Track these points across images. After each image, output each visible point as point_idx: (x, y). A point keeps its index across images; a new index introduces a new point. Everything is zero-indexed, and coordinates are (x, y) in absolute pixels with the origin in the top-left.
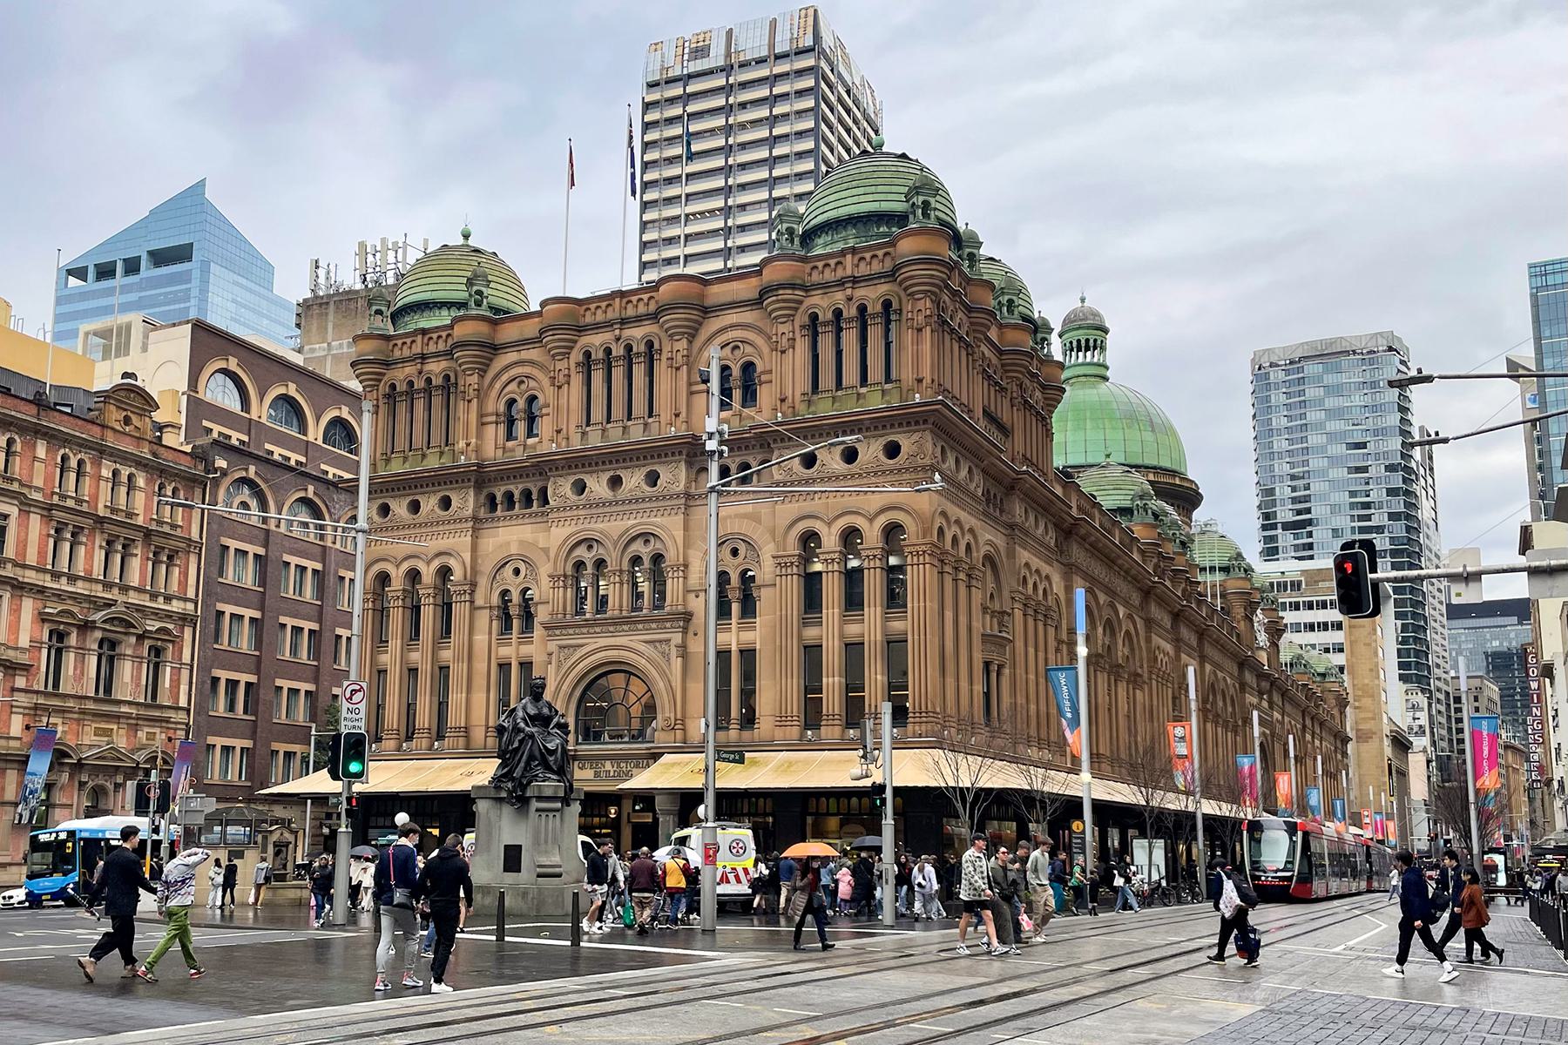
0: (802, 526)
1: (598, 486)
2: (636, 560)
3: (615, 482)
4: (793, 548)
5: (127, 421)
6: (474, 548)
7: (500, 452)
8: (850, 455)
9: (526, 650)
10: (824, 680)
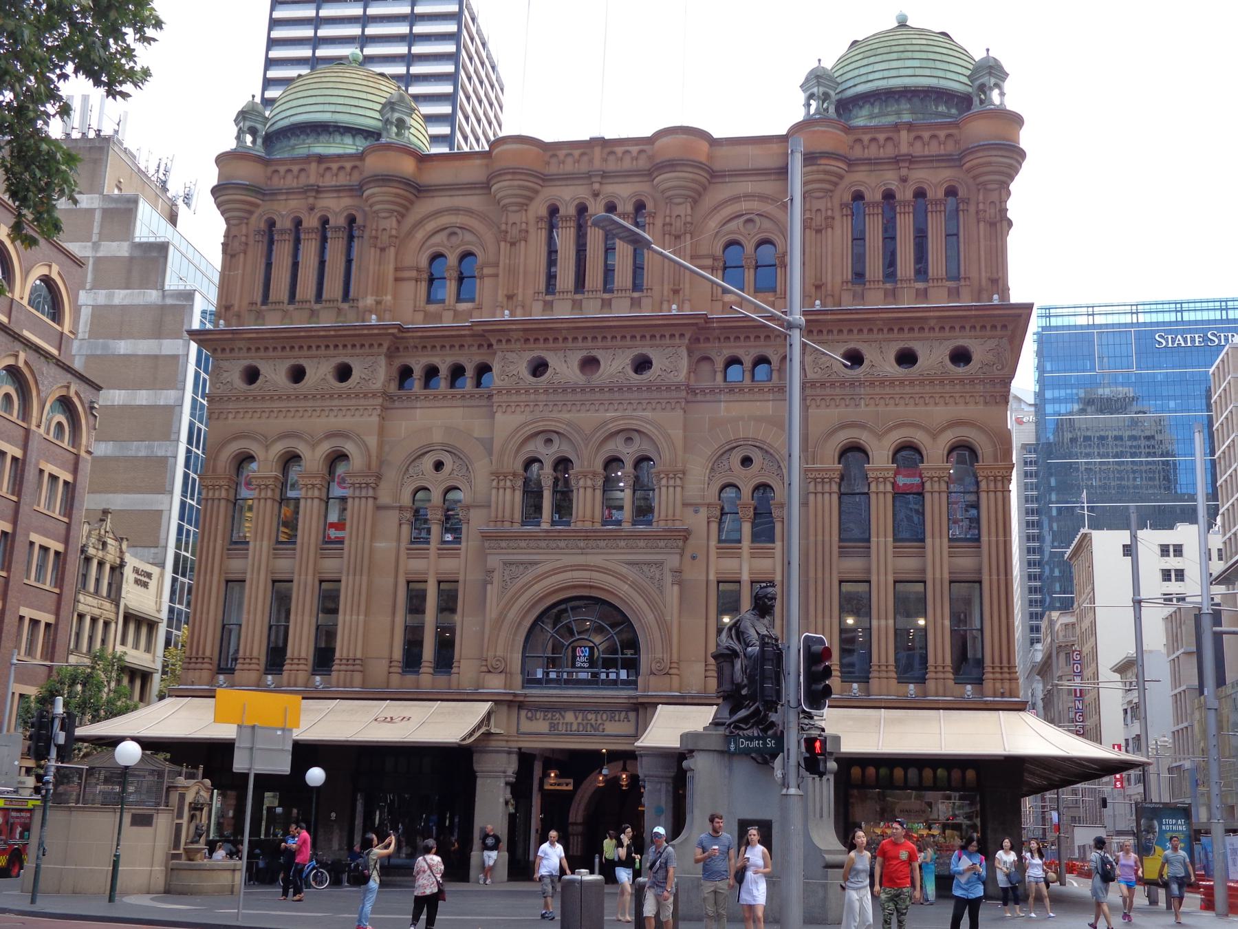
0: (843, 437)
2: (613, 462)
3: (590, 364)
4: (829, 462)
6: (382, 431)
7: (420, 316)
8: (906, 358)
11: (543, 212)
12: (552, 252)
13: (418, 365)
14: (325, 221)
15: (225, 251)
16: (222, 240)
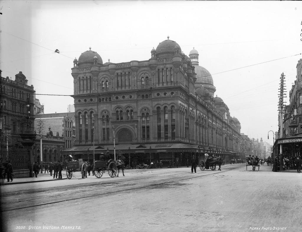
1: (120, 98)
4: (155, 109)
5: (21, 81)
6: (97, 109)
9: (108, 126)
10: (161, 132)
11: (116, 74)
12: (118, 81)
14: (87, 77)
15: (74, 83)
16: (73, 81)
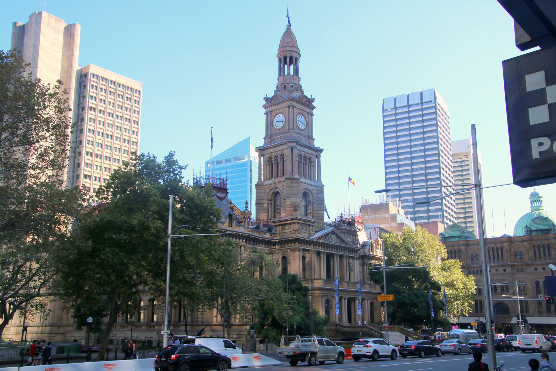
3: (497, 270)
13: (472, 270)
